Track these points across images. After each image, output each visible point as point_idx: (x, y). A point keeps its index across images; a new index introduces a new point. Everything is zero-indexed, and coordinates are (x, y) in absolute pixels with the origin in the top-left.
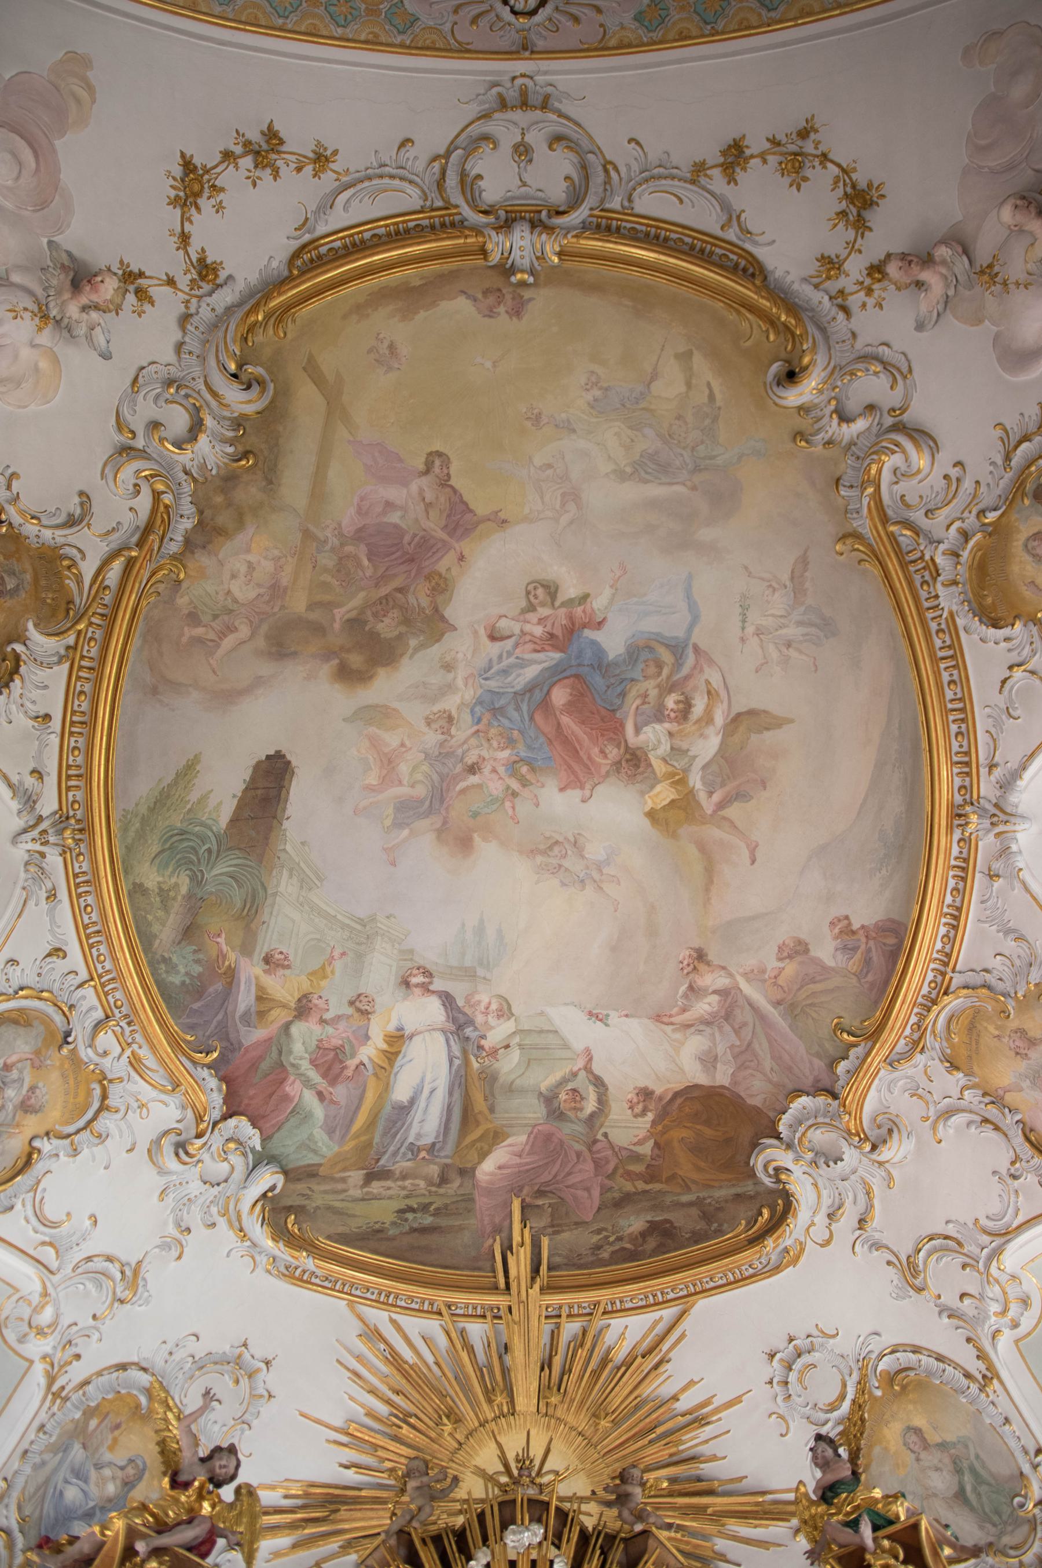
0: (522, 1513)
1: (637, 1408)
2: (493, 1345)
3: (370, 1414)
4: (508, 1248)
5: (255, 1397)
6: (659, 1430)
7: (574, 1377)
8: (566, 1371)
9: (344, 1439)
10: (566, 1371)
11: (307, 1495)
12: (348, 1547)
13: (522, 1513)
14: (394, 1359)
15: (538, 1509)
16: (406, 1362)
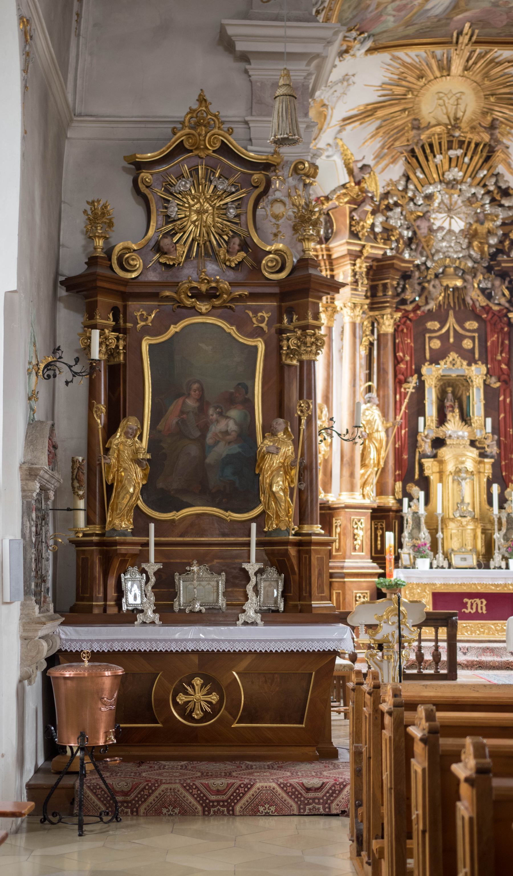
0: (455, 145)
1: (501, 76)
2: (445, 55)
3: (391, 79)
4: (460, 33)
5: (349, 85)
6: (508, 84)
7: (478, 66)
8: (475, 63)
9: (380, 88)
10: (475, 63)
11: (365, 108)
12: (378, 118)
13: (455, 145)
14: (404, 64)
15: (461, 144)
16: (408, 63)
